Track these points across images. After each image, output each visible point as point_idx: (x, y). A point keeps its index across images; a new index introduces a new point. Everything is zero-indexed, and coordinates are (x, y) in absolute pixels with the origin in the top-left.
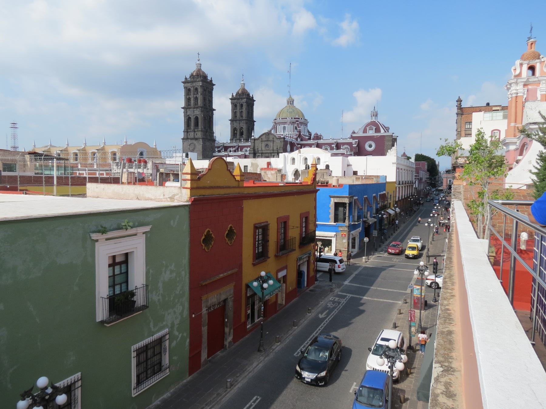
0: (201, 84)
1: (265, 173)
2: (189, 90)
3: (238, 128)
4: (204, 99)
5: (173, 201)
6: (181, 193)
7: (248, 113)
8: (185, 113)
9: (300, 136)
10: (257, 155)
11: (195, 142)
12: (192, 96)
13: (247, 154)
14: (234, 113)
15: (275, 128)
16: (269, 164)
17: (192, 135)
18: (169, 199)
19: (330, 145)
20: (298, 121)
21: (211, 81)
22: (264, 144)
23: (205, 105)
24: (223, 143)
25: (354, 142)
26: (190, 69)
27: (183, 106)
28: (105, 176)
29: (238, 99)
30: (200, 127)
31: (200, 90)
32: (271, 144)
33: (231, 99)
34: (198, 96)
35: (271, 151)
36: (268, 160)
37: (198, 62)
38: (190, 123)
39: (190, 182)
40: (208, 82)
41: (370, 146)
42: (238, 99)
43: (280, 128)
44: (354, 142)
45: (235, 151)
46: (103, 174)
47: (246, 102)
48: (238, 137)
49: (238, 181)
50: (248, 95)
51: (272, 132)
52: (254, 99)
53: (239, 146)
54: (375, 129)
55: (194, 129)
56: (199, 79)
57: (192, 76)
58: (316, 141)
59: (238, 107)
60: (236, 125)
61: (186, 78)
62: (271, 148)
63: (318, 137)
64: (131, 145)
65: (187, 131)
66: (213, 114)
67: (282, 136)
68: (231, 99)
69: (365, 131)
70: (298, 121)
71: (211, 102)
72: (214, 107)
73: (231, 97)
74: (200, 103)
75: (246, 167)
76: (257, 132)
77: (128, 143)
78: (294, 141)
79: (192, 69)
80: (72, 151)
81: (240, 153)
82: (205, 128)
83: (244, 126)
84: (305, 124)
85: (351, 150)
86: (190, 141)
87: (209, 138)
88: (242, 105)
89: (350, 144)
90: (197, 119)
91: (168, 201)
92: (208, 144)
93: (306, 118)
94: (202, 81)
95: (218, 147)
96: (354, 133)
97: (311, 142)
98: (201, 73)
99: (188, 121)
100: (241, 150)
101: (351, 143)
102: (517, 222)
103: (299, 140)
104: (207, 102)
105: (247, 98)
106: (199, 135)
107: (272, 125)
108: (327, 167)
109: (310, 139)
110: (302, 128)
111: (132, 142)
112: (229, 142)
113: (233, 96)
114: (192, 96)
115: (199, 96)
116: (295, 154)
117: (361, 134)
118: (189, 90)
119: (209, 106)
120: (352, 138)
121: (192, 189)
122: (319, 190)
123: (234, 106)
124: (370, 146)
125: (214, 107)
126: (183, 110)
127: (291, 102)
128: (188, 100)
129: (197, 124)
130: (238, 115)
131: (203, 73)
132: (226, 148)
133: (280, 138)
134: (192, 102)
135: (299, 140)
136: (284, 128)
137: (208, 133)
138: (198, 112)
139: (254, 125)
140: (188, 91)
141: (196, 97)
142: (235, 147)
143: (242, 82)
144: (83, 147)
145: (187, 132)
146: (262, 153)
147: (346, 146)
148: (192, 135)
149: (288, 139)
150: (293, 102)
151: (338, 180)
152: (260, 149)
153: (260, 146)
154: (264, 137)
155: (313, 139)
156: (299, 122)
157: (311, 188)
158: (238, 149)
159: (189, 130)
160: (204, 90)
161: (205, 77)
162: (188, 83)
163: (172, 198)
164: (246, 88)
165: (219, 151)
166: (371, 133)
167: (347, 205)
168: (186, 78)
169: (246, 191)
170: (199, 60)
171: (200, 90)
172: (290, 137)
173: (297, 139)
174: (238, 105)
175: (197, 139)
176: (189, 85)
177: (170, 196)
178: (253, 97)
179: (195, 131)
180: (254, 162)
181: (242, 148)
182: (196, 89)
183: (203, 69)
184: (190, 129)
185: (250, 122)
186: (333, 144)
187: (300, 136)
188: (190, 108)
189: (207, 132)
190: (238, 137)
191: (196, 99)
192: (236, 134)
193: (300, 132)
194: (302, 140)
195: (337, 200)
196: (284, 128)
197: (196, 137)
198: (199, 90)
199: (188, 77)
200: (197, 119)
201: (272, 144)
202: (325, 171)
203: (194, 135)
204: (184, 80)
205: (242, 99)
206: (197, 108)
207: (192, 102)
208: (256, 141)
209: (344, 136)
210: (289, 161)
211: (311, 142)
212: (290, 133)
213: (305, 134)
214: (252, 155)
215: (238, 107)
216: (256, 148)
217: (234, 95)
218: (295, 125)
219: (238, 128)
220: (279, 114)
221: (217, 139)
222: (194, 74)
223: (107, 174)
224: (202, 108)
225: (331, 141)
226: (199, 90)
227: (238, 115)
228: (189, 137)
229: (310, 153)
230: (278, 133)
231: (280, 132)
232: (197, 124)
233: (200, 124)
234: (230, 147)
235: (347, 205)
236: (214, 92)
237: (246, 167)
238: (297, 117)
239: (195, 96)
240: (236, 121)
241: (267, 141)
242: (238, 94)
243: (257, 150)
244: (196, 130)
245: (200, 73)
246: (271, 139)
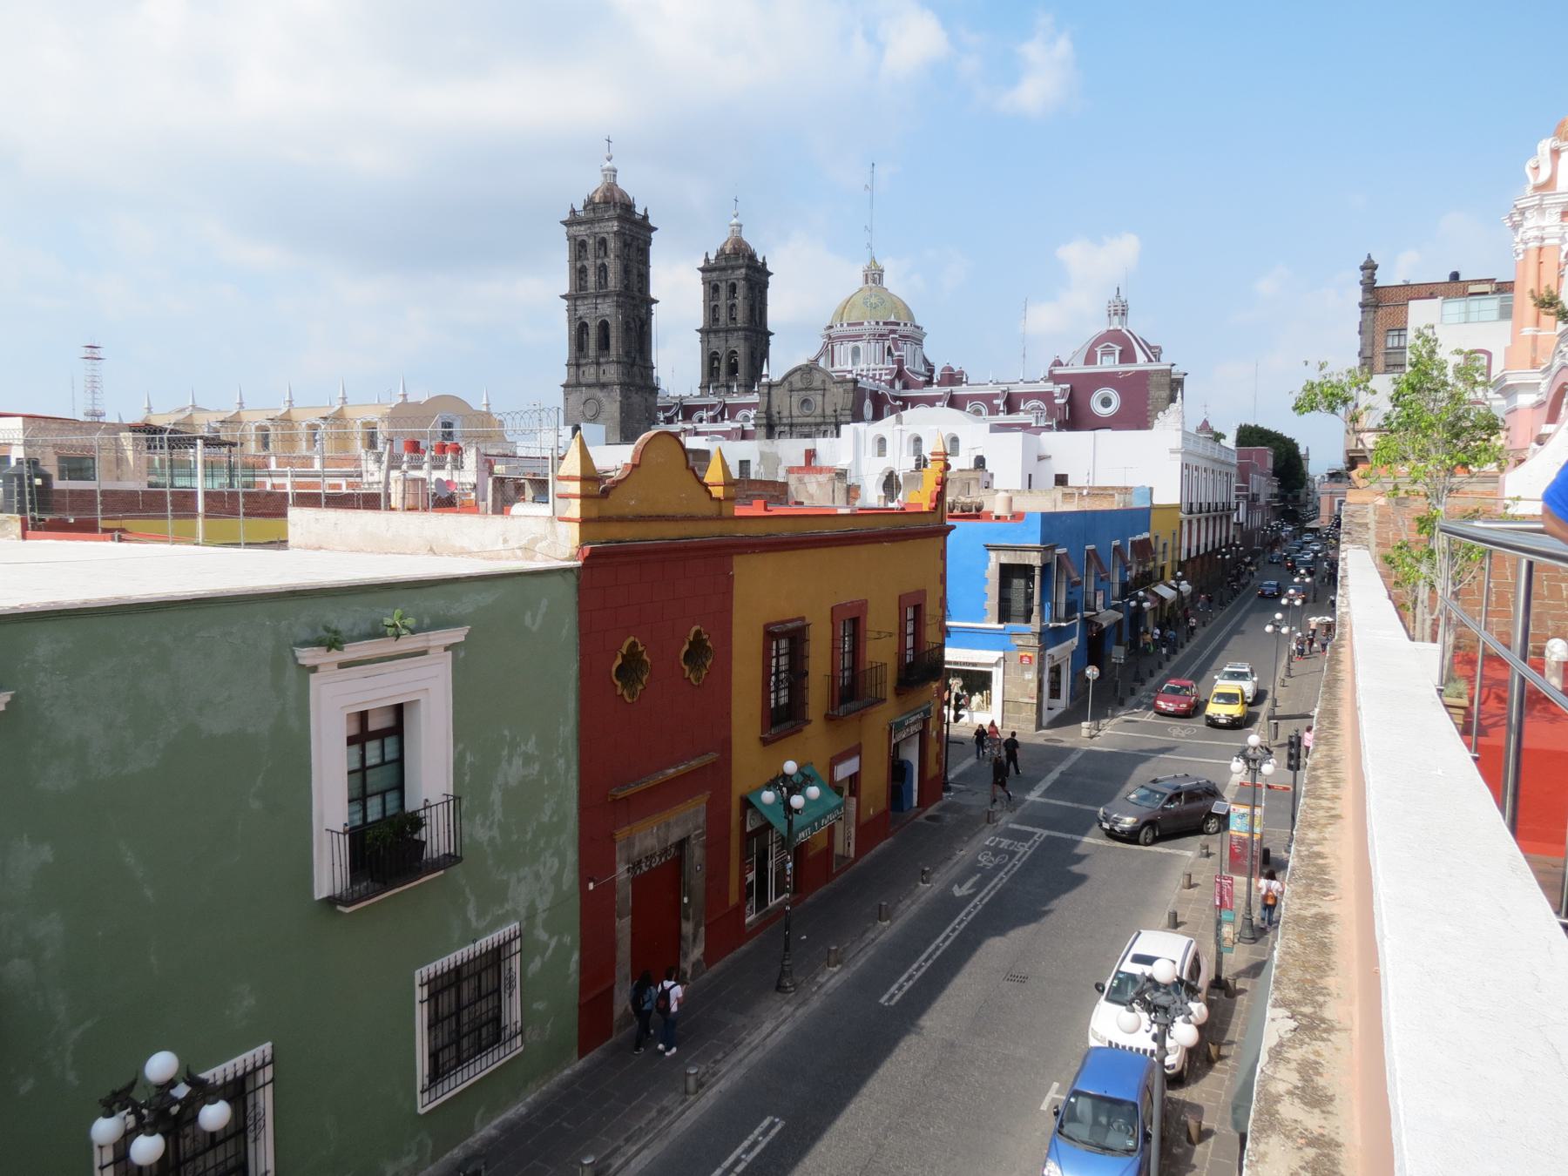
1: (800, 480)
2: (583, 244)
3: (722, 353)
4: (626, 271)
5: (532, 559)
6: (554, 533)
7: (752, 309)
8: (572, 310)
9: (900, 374)
10: (777, 429)
11: (599, 394)
12: (590, 264)
13: (749, 426)
14: (712, 311)
15: (828, 350)
16: (810, 455)
17: (590, 374)
18: (519, 553)
19: (988, 399)
20: (894, 332)
21: (646, 217)
22: (796, 398)
23: (627, 287)
24: (682, 398)
25: (1057, 390)
26: (585, 185)
27: (566, 290)
28: (344, 490)
29: (723, 269)
30: (613, 351)
31: (612, 244)
32: (817, 398)
33: (703, 270)
34: (606, 261)
35: (819, 420)
36: (807, 443)
37: (608, 164)
38: (586, 341)
39: (578, 501)
40: (635, 223)
41: (1106, 402)
42: (723, 269)
43: (843, 351)
44: (1057, 390)
45: (714, 420)
46: (339, 486)
47: (747, 278)
48: (723, 378)
49: (719, 499)
50: (752, 257)
51: (822, 363)
52: (769, 268)
53: (725, 405)
54: (1121, 352)
55: (597, 357)
56: (612, 213)
57: (590, 204)
58: (948, 389)
59: (723, 293)
60: (718, 344)
61: (573, 211)
62: (819, 411)
63: (952, 378)
64: (417, 404)
65: (576, 364)
66: (649, 313)
67: (849, 376)
68: (703, 270)
69: (1090, 359)
70: (894, 332)
71: (644, 278)
72: (653, 294)
73: (702, 264)
74: (613, 281)
75: (744, 464)
76: (780, 362)
77: (410, 400)
78: (883, 388)
79: (589, 184)
80: (254, 418)
81: (727, 425)
82: (627, 354)
83: (739, 346)
84: (916, 338)
85: (1050, 415)
87: (638, 380)
88: (733, 288)
89: (1047, 397)
90: (604, 327)
91: (517, 558)
92: (636, 398)
93: (918, 323)
94: (619, 218)
95: (666, 409)
96: (1058, 363)
97: (934, 391)
98: (617, 196)
99: (580, 332)
100: (732, 417)
101: (1051, 393)
102: (1530, 564)
103: (898, 385)
104: (634, 278)
105: (748, 267)
106: (612, 373)
107: (818, 344)
108: (980, 462)
109: (929, 382)
110: (906, 351)
111: (419, 395)
112: (697, 392)
113: (707, 260)
114: (590, 264)
116: (887, 426)
117: (1079, 368)
118: (583, 244)
119: (640, 290)
120: (1055, 378)
121: (584, 521)
122: (953, 527)
123: (712, 289)
124: (1106, 402)
125: (654, 293)
126: (565, 303)
127: (875, 276)
128: (579, 274)
129: (604, 344)
130: (723, 314)
131: (623, 194)
132: (688, 412)
133: (844, 381)
134: (592, 278)
135: (898, 385)
136: (856, 352)
137: (636, 369)
138: (607, 309)
139: (767, 343)
140: (579, 248)
141: (604, 265)
142: (712, 407)
143: (735, 221)
144: (284, 410)
145: (578, 366)
146: (791, 425)
147: (1034, 403)
148: (590, 374)
149: (866, 384)
150: (881, 276)
151: (1011, 500)
152: (785, 413)
153: (786, 405)
154: (796, 377)
155: (939, 384)
156: (898, 333)
157: (932, 523)
158: (722, 413)
159: (583, 361)
160: (626, 245)
161: (628, 207)
162: (580, 223)
163: (528, 550)
164: (746, 237)
165: (669, 421)
166: (1109, 364)
167: (1037, 571)
168: (573, 211)
169: (741, 531)
170: (609, 159)
171: (612, 244)
172: (873, 378)
173: (891, 384)
174: (723, 286)
175: (603, 386)
176: (581, 231)
177: (523, 543)
178: (764, 264)
179: (598, 364)
180: (767, 450)
181: (733, 410)
182: (603, 243)
183: (623, 183)
185: (758, 337)
186: (996, 396)
187: (900, 374)
188: (584, 298)
189: (632, 365)
190: (723, 378)
191: (603, 269)
192: (717, 369)
193: (900, 362)
194: (906, 387)
195: (1007, 558)
196: (856, 352)
197: (603, 379)
198: (612, 244)
199: (579, 207)
200: (604, 327)
201: (819, 398)
202: (973, 475)
204: (566, 217)
205: (733, 268)
206: (605, 296)
207: (592, 278)
208: (774, 392)
209: (1029, 374)
210: (870, 447)
211: (934, 391)
212: (872, 366)
213: (917, 369)
214: (762, 431)
215: (723, 293)
216: (774, 410)
217: (712, 257)
218: (887, 344)
219: (722, 353)
220: (840, 314)
221: (663, 386)
223: (349, 485)
225: (990, 389)
226: (612, 244)
227: (723, 314)
228: (583, 380)
229: (931, 424)
230: (837, 367)
231: (844, 364)
232: (604, 344)
233: (613, 341)
234: (700, 408)
235: (1037, 571)
236: (654, 250)
237: (744, 464)
238: (892, 319)
239: (599, 262)
240: (716, 332)
241: (806, 389)
242: (721, 253)
243: (776, 416)
246: (817, 383)
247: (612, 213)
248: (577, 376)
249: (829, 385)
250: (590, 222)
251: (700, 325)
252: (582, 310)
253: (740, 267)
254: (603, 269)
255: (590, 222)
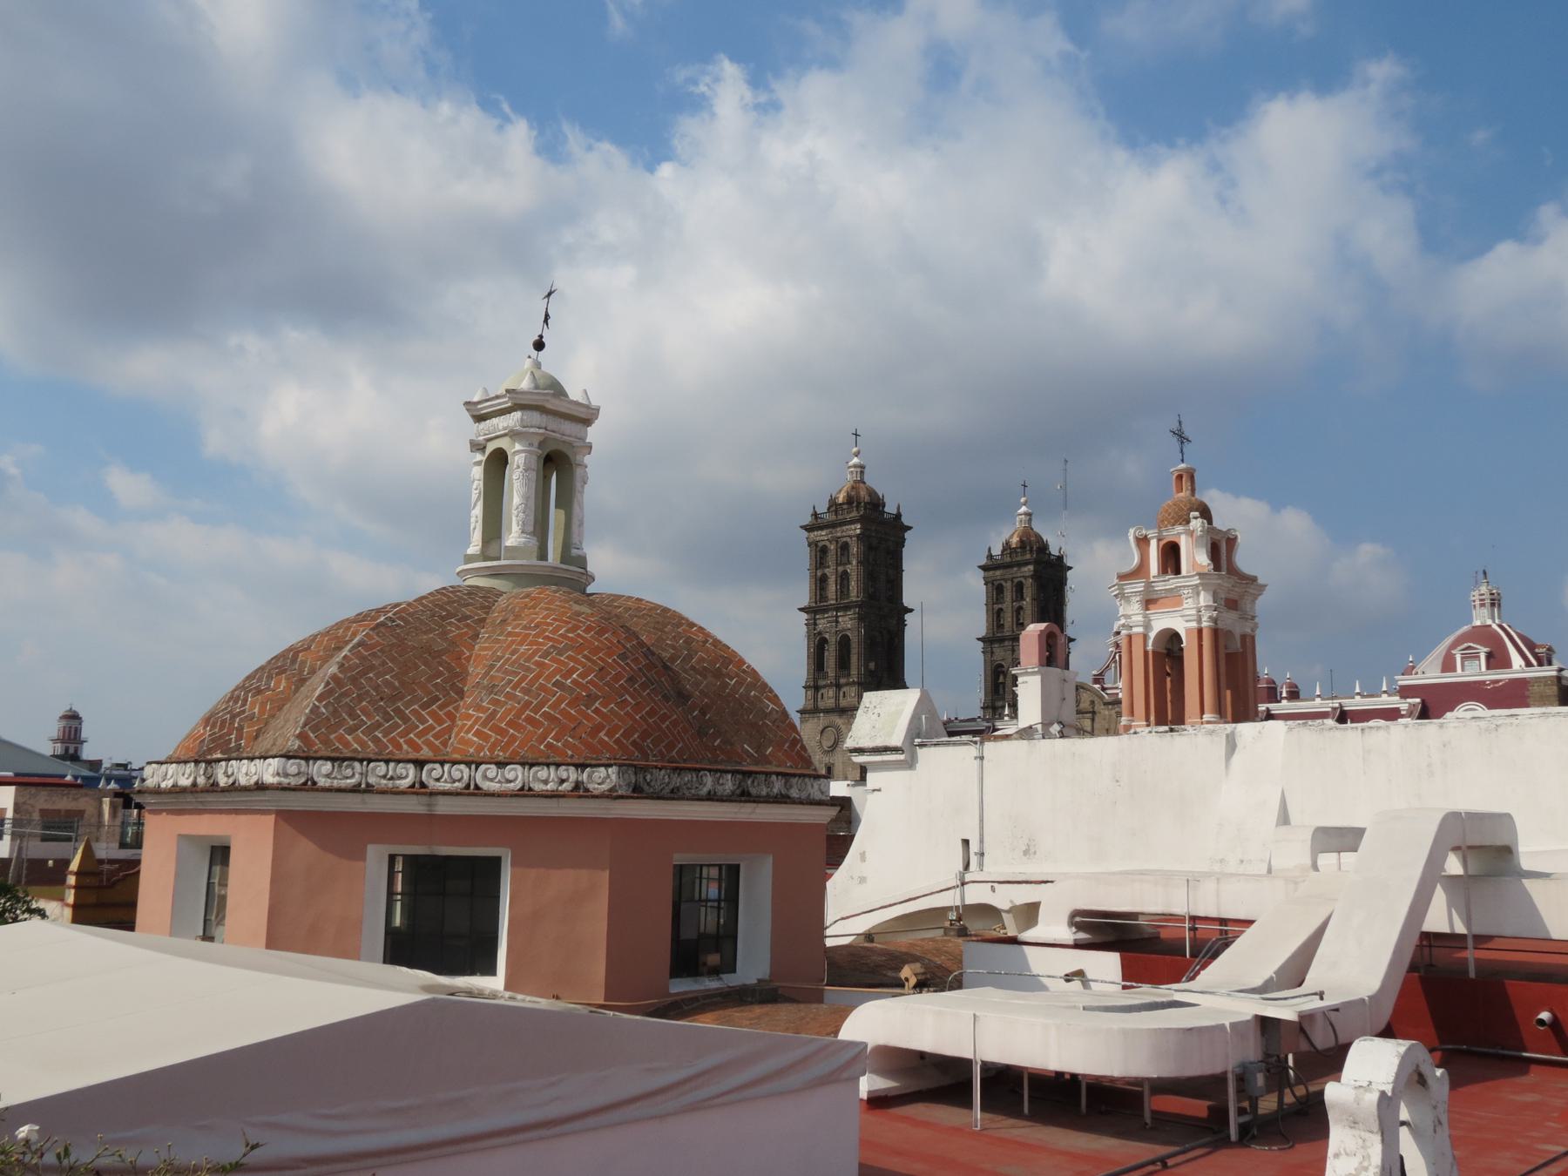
0: (857, 529)
8: (811, 624)
17: (828, 698)
21: (898, 516)
27: (805, 602)
30: (854, 672)
33: (984, 568)
34: (849, 568)
40: (884, 523)
47: (1036, 576)
50: (1043, 548)
54: (1489, 656)
55: (837, 677)
57: (834, 505)
61: (815, 515)
66: (902, 624)
68: (984, 568)
73: (984, 561)
86: (823, 720)
88: (1019, 588)
94: (861, 520)
98: (863, 493)
99: (818, 647)
113: (990, 556)
115: (853, 568)
125: (908, 599)
126: (805, 616)
128: (820, 583)
131: (872, 493)
134: (832, 588)
138: (847, 622)
140: (820, 554)
141: (845, 572)
145: (817, 688)
148: (828, 698)
159: (822, 683)
161: (876, 504)
162: (821, 528)
170: (857, 454)
174: (1008, 585)
178: (1060, 558)
179: (838, 686)
182: (845, 548)
183: (872, 481)
184: (826, 677)
188: (825, 611)
191: (844, 578)
199: (822, 508)
200: (844, 643)
203: (837, 698)
204: (808, 520)
205: (1020, 565)
206: (846, 608)
207: (832, 588)
222: (840, 500)
224: (860, 607)
228: (821, 705)
232: (843, 664)
233: (854, 659)
236: (906, 552)
239: (840, 569)
240: (1001, 640)
244: (842, 681)
245: (858, 494)
247: (854, 514)
248: (815, 700)
249: (1099, 707)
250: (832, 526)
251: (982, 632)
252: (822, 624)
253: (1026, 563)
254: (844, 578)
255: (832, 526)
